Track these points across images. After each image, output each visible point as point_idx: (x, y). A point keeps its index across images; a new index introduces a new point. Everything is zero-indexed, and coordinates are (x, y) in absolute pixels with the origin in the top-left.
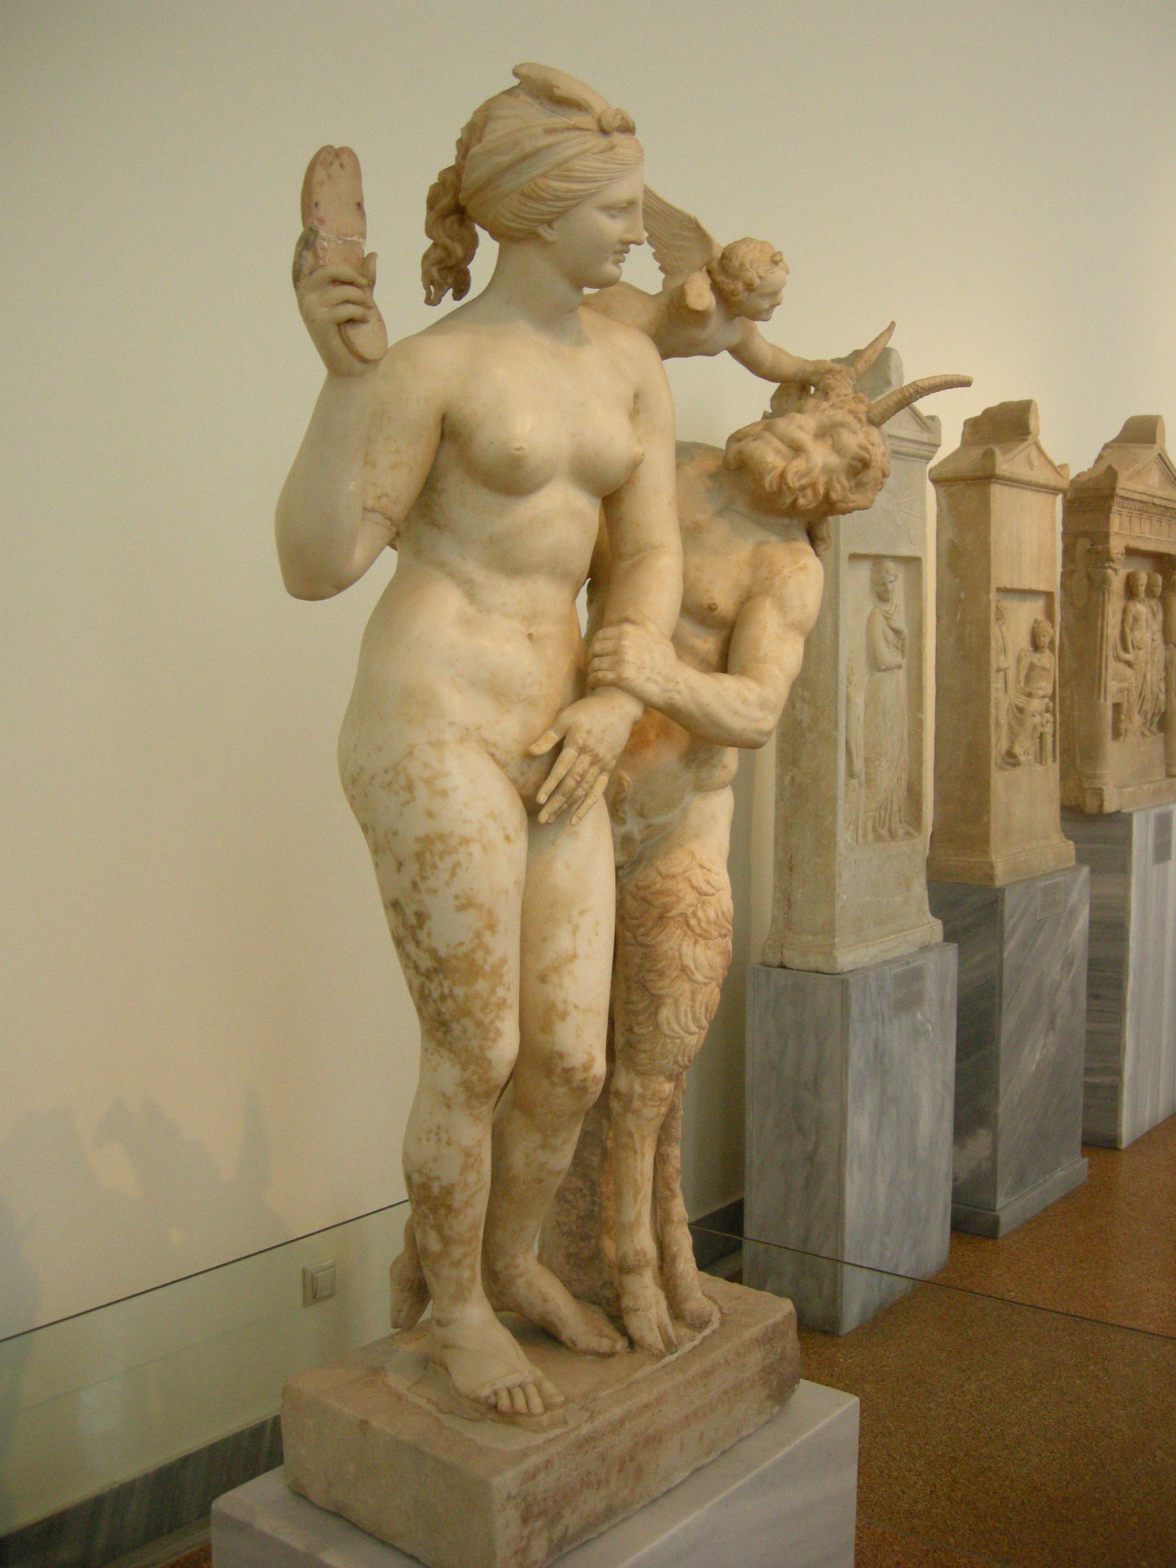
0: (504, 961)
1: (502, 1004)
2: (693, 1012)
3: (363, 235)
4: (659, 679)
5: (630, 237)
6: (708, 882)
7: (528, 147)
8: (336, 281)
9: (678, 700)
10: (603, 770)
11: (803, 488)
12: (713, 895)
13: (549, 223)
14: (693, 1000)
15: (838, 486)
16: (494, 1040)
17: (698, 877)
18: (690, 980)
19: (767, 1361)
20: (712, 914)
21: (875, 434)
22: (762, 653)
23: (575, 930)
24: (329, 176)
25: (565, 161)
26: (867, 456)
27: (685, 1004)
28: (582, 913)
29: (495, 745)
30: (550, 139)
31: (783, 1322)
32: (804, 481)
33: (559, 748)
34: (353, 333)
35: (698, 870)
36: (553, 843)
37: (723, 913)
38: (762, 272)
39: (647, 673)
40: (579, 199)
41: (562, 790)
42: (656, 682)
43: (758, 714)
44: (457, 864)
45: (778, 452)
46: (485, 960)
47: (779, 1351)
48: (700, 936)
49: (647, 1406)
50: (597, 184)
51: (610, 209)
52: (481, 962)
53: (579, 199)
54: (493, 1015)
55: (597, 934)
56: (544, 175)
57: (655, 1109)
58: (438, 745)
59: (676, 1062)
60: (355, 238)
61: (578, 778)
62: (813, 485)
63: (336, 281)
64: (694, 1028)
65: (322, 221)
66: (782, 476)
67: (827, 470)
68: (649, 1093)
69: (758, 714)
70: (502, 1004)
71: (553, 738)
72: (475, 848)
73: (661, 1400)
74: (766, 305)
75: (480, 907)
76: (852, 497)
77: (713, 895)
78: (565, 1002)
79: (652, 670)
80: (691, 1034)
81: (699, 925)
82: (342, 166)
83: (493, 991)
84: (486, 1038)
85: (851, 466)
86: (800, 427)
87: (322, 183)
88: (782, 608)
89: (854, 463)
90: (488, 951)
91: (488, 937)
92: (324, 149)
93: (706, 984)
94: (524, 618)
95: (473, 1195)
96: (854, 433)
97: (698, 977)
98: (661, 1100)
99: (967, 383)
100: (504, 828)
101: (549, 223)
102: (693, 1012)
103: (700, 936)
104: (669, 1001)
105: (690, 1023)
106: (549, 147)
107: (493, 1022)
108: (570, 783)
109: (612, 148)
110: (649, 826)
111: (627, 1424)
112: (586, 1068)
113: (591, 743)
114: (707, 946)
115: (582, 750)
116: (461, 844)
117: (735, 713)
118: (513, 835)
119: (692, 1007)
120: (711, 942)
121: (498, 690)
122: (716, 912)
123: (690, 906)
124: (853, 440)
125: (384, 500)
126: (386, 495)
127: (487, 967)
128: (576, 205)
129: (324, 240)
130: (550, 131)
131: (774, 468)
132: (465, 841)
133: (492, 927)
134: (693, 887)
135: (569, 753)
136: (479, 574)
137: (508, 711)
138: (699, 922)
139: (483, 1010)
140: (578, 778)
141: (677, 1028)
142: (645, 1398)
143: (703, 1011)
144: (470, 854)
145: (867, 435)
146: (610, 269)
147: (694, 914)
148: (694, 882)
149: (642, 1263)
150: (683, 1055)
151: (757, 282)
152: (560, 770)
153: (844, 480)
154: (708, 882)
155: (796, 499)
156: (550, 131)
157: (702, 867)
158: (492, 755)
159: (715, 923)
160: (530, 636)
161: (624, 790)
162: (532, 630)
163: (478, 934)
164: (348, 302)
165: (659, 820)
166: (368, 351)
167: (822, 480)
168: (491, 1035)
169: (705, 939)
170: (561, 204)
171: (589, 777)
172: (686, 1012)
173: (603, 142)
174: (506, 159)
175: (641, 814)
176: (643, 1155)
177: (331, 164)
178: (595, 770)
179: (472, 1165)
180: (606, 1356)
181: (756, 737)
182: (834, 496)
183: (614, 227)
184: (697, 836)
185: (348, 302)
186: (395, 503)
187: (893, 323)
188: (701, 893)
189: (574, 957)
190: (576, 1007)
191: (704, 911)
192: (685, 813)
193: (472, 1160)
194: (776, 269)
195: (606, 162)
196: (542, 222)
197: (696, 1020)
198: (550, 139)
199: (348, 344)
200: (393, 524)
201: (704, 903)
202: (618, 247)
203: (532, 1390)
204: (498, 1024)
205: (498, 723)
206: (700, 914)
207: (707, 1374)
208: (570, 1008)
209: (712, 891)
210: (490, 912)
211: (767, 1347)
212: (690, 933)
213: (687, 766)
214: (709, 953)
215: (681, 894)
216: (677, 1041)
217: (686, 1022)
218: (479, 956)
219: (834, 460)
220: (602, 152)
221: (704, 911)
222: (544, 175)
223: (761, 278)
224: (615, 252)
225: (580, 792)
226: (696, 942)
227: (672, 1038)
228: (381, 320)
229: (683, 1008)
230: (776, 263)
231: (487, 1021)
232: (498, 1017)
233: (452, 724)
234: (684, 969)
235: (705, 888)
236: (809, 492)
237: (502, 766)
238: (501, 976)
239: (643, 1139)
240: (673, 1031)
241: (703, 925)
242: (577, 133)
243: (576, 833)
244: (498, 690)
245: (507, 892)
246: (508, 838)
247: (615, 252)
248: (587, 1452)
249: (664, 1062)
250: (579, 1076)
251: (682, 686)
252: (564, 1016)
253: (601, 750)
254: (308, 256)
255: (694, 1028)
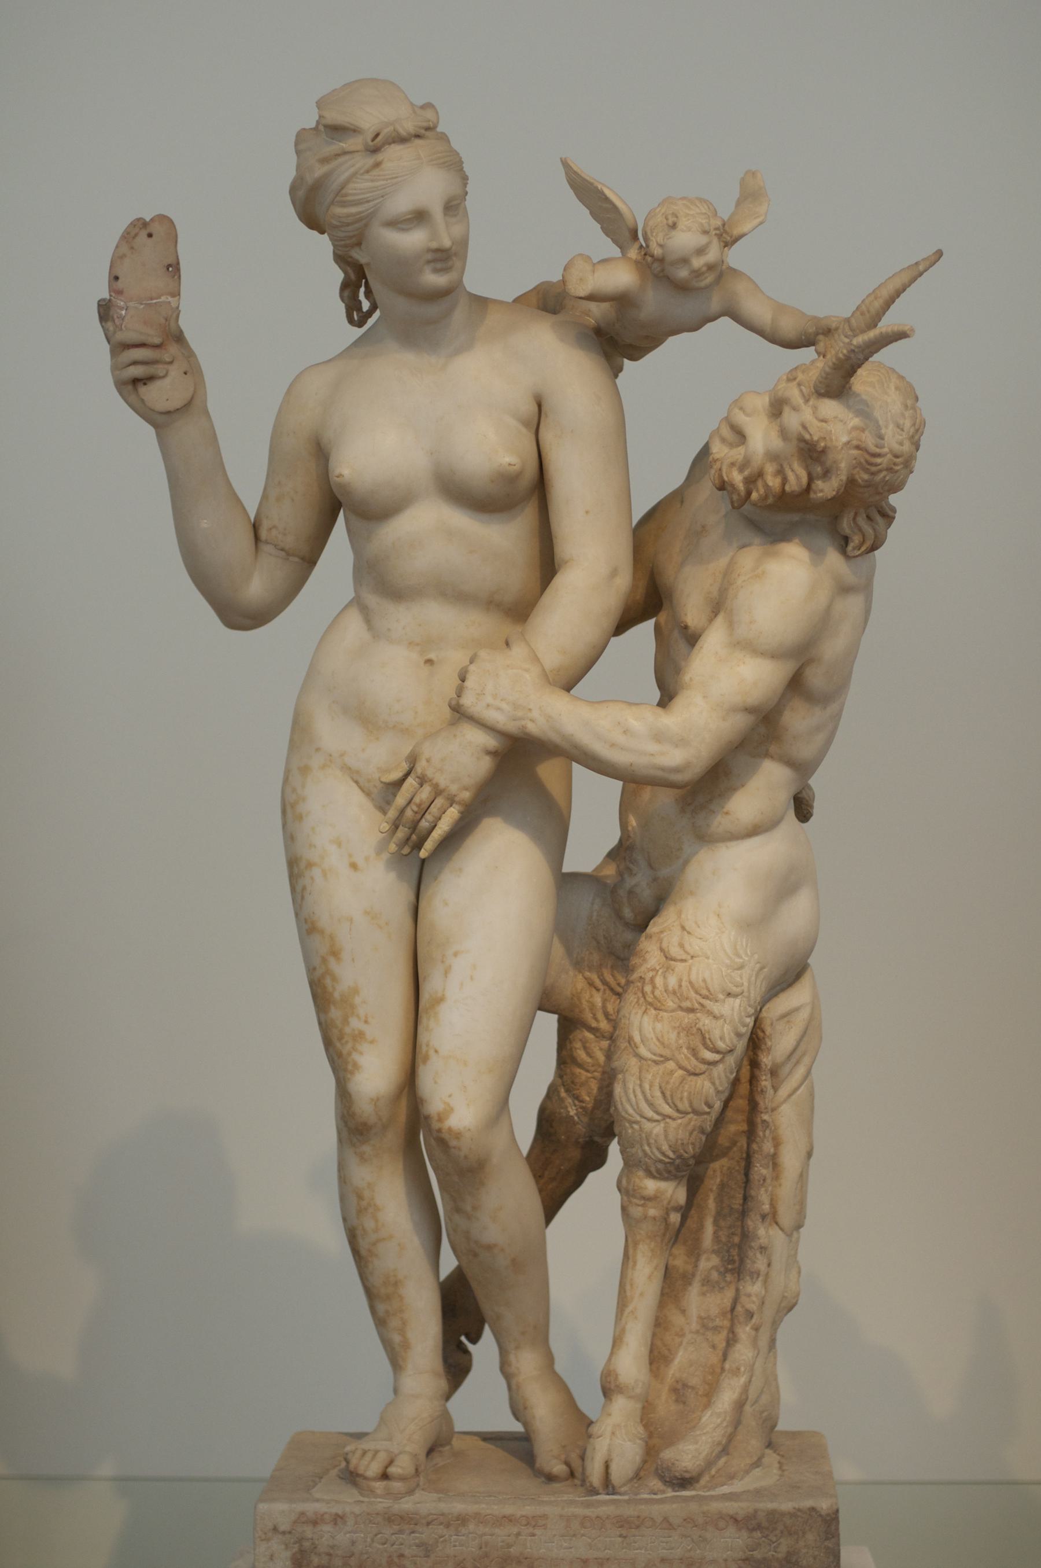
0: (355, 991)
1: (359, 1036)
2: (643, 1093)
3: (177, 294)
4: (504, 706)
5: (434, 245)
6: (681, 946)
7: (310, 179)
8: (127, 346)
9: (533, 728)
10: (452, 801)
11: (751, 481)
12: (683, 961)
13: (359, 244)
14: (640, 1080)
15: (791, 477)
16: (352, 1073)
17: (672, 942)
18: (638, 1056)
19: (757, 1554)
20: (672, 981)
21: (830, 408)
22: (687, 678)
23: (447, 972)
24: (132, 248)
25: (343, 186)
26: (807, 437)
27: (632, 1083)
28: (456, 954)
29: (358, 772)
30: (326, 168)
31: (793, 1515)
32: (746, 473)
33: (407, 775)
34: (142, 390)
35: (677, 931)
36: (436, 879)
37: (690, 983)
38: (660, 239)
39: (489, 699)
40: (364, 222)
41: (404, 820)
42: (498, 709)
43: (652, 747)
44: (304, 888)
45: (723, 440)
46: (334, 988)
47: (783, 1549)
48: (651, 1004)
49: (510, 1519)
50: (371, 204)
51: (395, 223)
52: (330, 989)
53: (364, 222)
54: (349, 1046)
55: (472, 978)
56: (332, 203)
57: (640, 1209)
58: (305, 770)
59: (644, 1151)
60: (163, 299)
61: (415, 809)
62: (760, 474)
63: (127, 346)
64: (650, 1114)
65: (120, 292)
66: (720, 470)
67: (773, 457)
68: (631, 1187)
69: (652, 747)
70: (359, 1036)
71: (405, 767)
72: (316, 872)
73: (532, 1522)
74: (683, 273)
75: (322, 932)
76: (819, 484)
77: (683, 961)
78: (427, 1045)
79: (495, 696)
80: (649, 1120)
81: (653, 992)
82: (150, 235)
83: (346, 1021)
84: (346, 1070)
85: (802, 449)
86: (741, 409)
87: (122, 257)
88: (731, 625)
89: (802, 445)
90: (334, 979)
91: (332, 962)
92: (133, 224)
93: (656, 1062)
94: (411, 644)
95: (374, 1244)
96: (795, 409)
97: (643, 1051)
98: (644, 1198)
99: (901, 335)
100: (350, 856)
101: (359, 244)
102: (643, 1093)
103: (651, 1004)
104: (620, 1076)
105: (644, 1106)
106: (327, 176)
107: (349, 1054)
108: (409, 813)
109: (377, 165)
110: (655, 880)
111: (471, 1527)
112: (440, 1119)
113: (429, 773)
114: (657, 1019)
115: (422, 781)
116: (306, 867)
117: (613, 745)
118: (360, 862)
119: (641, 1086)
120: (662, 1013)
121: (366, 717)
122: (680, 980)
123: (650, 970)
124: (792, 420)
125: (274, 532)
126: (275, 527)
127: (337, 995)
128: (366, 225)
129: (122, 309)
130: (324, 161)
131: (716, 461)
132: (310, 865)
133: (335, 953)
134: (662, 950)
135: (410, 780)
136: (372, 600)
137: (377, 739)
138: (654, 987)
139: (340, 1039)
140: (415, 809)
141: (631, 1111)
142: (508, 1510)
143: (658, 1094)
144: (312, 878)
145: (815, 409)
146: (432, 279)
147: (652, 980)
148: (664, 945)
149: (612, 1386)
150: (649, 1145)
151: (657, 251)
152: (400, 800)
153: (796, 466)
154: (681, 946)
155: (749, 493)
156: (324, 161)
157: (683, 928)
158: (356, 782)
159: (674, 993)
160: (429, 662)
161: (632, 835)
162: (432, 656)
163: (324, 960)
164: (135, 363)
165: (664, 872)
166: (161, 405)
167: (770, 469)
168: (350, 1067)
169: (655, 1009)
170: (350, 228)
171: (434, 809)
172: (634, 1091)
173: (370, 161)
174: (301, 193)
175: (651, 866)
176: (635, 1263)
177: (136, 235)
178: (439, 802)
179: (366, 1209)
180: (550, 1478)
181: (659, 773)
182: (787, 488)
183: (414, 240)
184: (692, 893)
185: (135, 363)
186: (285, 534)
187: (939, 254)
188: (668, 958)
189: (440, 1000)
190: (436, 1051)
191: (665, 977)
192: (686, 863)
193: (364, 1203)
194: (674, 233)
195: (372, 181)
196: (353, 246)
197: (651, 1105)
198: (326, 168)
199: (142, 400)
200: (288, 554)
201: (668, 969)
202: (429, 256)
203: (382, 1457)
204: (355, 1056)
205: (363, 750)
206: (659, 981)
207: (623, 1523)
208: (431, 1052)
209: (684, 957)
210: (332, 938)
211: (758, 1534)
212: (642, 1000)
213: (683, 811)
214: (659, 1026)
215: (647, 956)
216: (636, 1127)
217: (637, 1104)
218: (328, 981)
219: (777, 443)
220: (367, 172)
221: (665, 977)
222: (332, 203)
223: (661, 246)
224: (429, 262)
225: (424, 824)
226: (645, 1012)
227: (631, 1122)
228: (193, 370)
229: (631, 1086)
230: (674, 226)
231: (345, 1052)
232: (354, 1049)
233: (318, 750)
234: (630, 1040)
235: (675, 951)
236: (760, 483)
237: (368, 794)
238: (353, 1007)
239: (636, 1244)
240: (626, 1112)
241: (657, 993)
242: (347, 157)
243: (460, 870)
244: (366, 717)
245: (351, 920)
246: (354, 866)
247: (429, 262)
248: (401, 1532)
249: (634, 1150)
250: (435, 1125)
251: (535, 714)
252: (426, 1059)
253: (442, 781)
254: (110, 325)
255: (650, 1114)
